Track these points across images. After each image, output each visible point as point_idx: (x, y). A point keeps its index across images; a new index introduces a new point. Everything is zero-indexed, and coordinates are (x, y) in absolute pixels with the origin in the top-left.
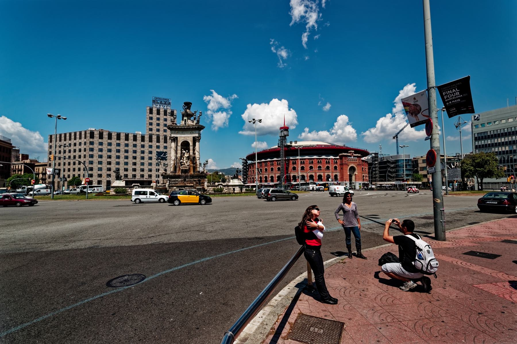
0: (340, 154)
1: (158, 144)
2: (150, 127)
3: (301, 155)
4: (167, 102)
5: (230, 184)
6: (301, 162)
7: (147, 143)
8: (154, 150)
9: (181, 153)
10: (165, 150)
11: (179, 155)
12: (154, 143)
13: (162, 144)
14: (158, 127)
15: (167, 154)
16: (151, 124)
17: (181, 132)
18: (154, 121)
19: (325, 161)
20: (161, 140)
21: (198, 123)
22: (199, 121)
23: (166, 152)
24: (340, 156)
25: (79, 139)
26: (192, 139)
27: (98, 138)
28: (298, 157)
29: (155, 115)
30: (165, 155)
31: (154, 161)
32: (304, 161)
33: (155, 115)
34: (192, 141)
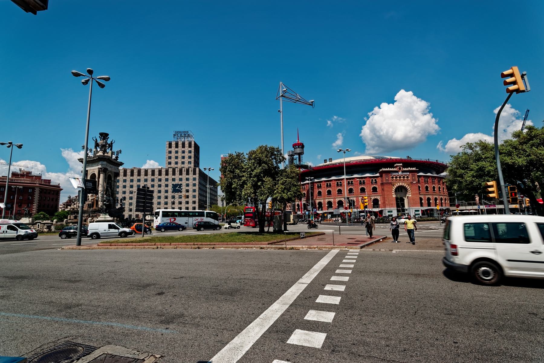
0: (381, 170)
1: (173, 177)
2: (169, 160)
3: (347, 174)
4: (186, 134)
6: (349, 182)
7: (163, 177)
8: (170, 183)
10: (180, 183)
12: (170, 176)
13: (177, 176)
14: (176, 160)
15: (182, 187)
16: (170, 158)
18: (173, 155)
19: (369, 181)
20: (183, 172)
23: (181, 184)
24: (380, 173)
27: (123, 176)
28: (344, 177)
29: (173, 149)
30: (180, 187)
31: (170, 194)
32: (364, 181)
33: (173, 149)
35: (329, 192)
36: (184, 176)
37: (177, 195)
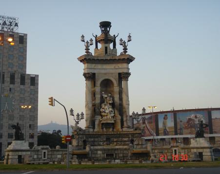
5: (191, 146)
9: (102, 97)
11: (98, 101)
22: (127, 49)
26: (117, 77)
34: (118, 80)
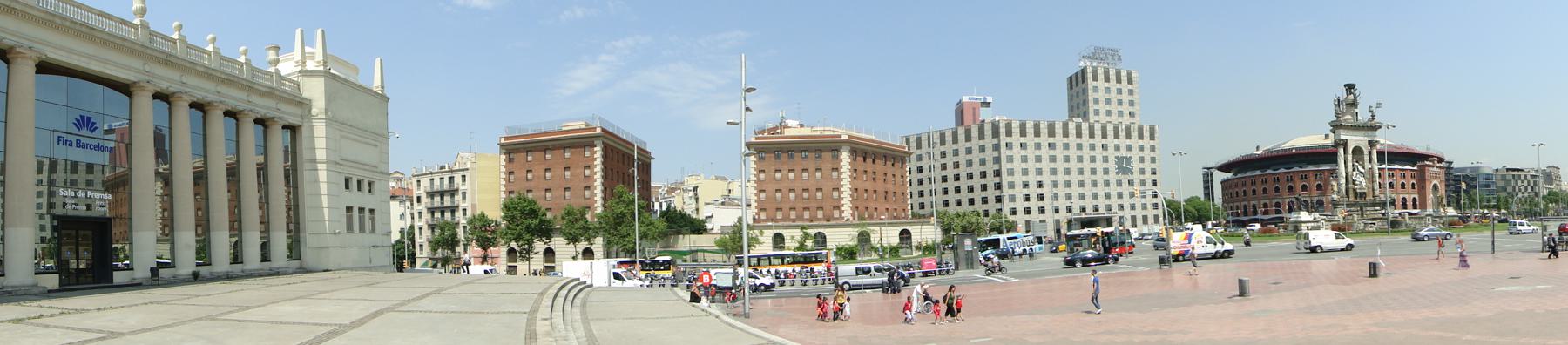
8: (1112, 154)
11: (1350, 169)
12: (1111, 141)
13: (1123, 141)
17: (1351, 132)
21: (1373, 119)
23: (1131, 158)
25: (980, 139)
31: (1112, 177)
35: (1403, 185)
36: (1135, 142)
37: (1125, 179)
